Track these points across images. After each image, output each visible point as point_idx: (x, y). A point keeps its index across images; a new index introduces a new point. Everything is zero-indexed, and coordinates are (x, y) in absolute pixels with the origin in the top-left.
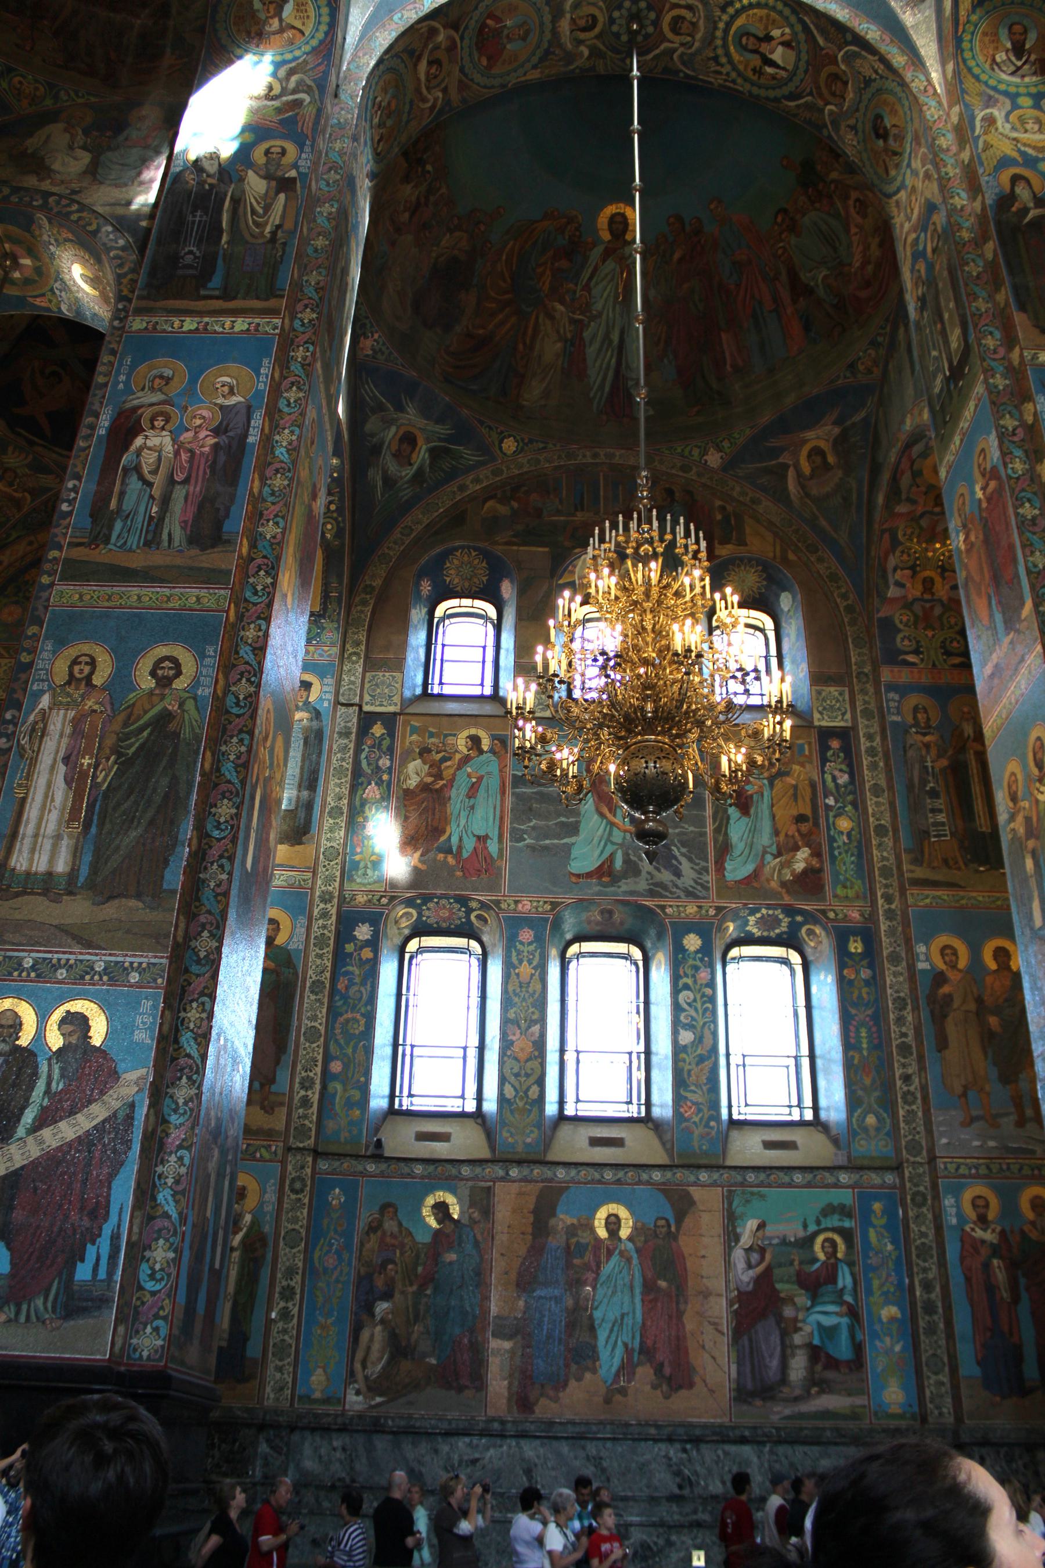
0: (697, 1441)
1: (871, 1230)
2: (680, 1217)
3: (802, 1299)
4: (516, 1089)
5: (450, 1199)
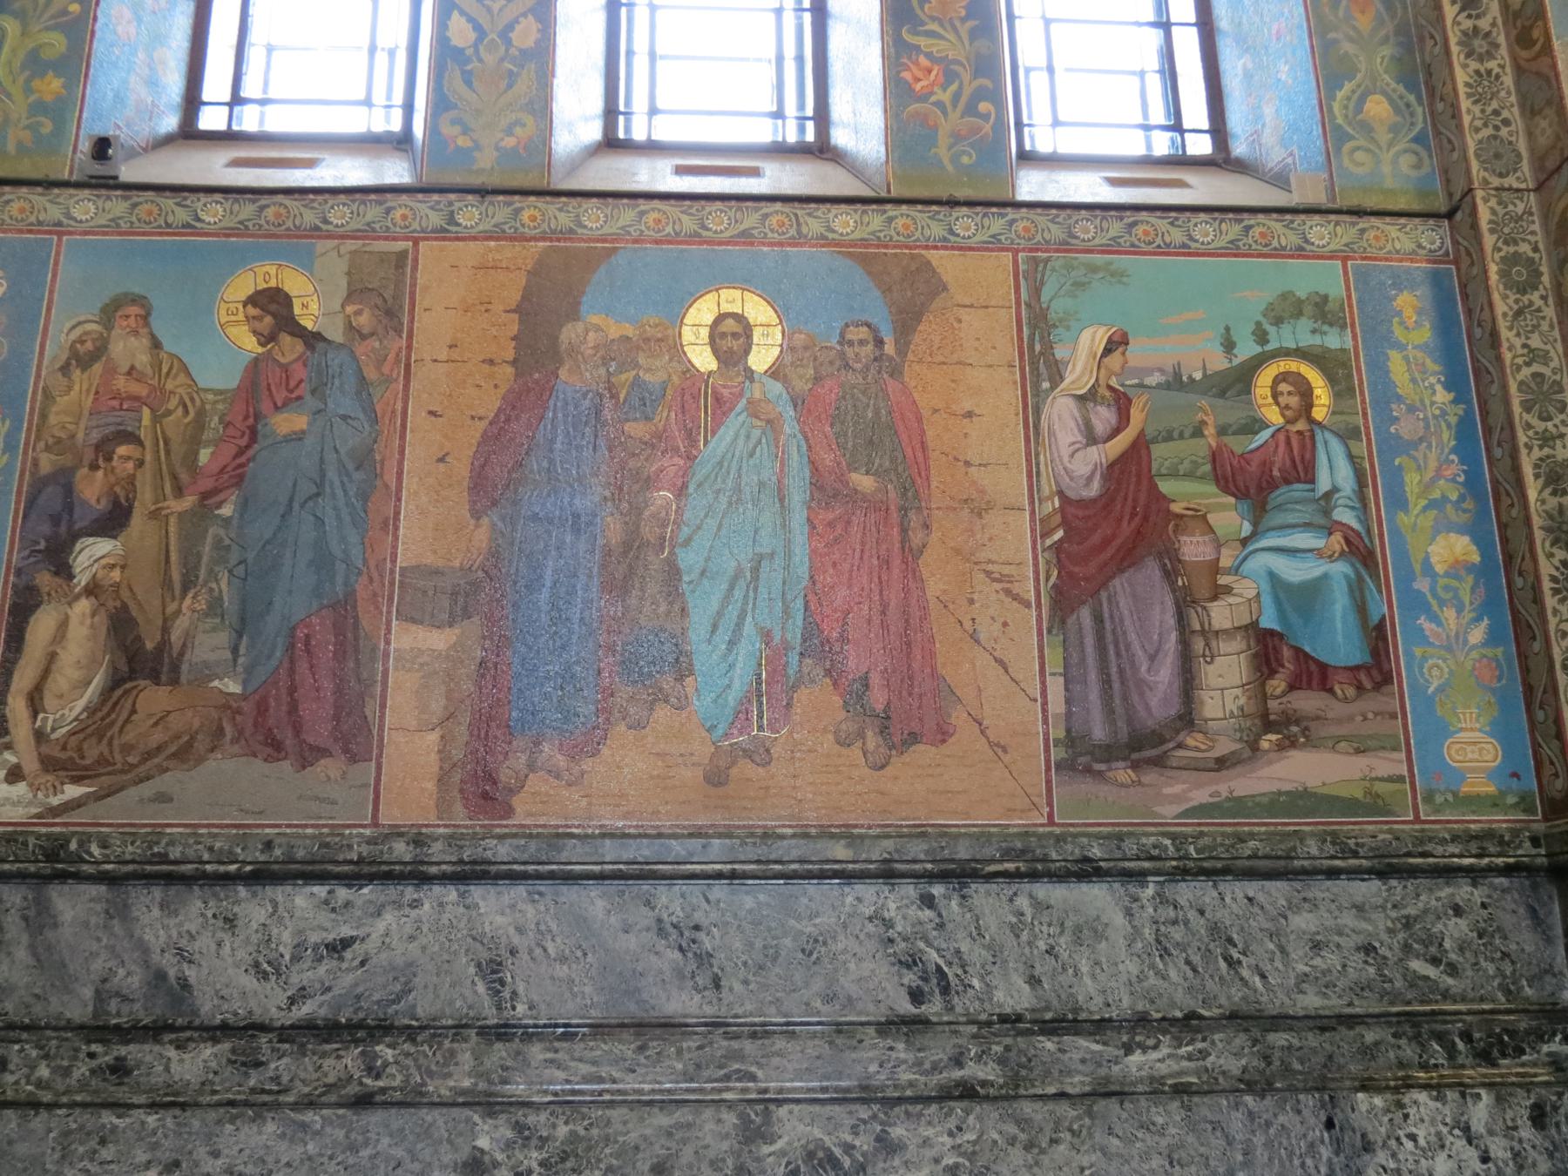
0: (961, 874)
1: (1395, 357)
2: (907, 321)
3: (1229, 518)
4: (478, 28)
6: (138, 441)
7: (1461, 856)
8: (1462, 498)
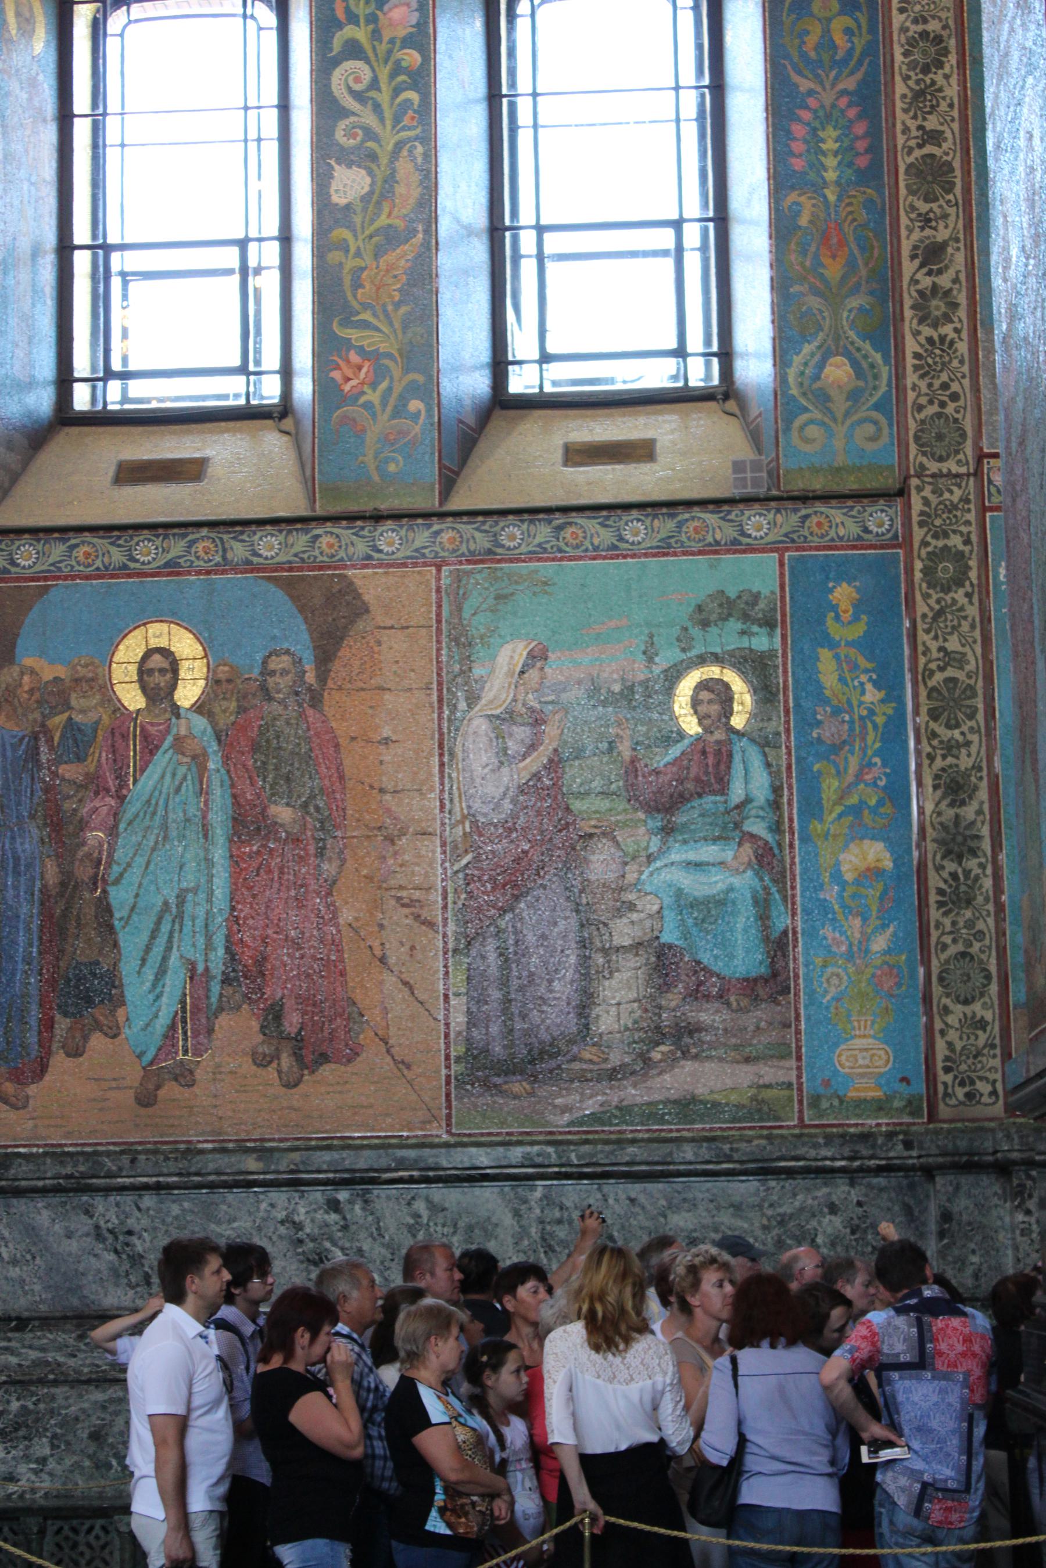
1: (825, 654)
7: (833, 1159)
8: (880, 803)
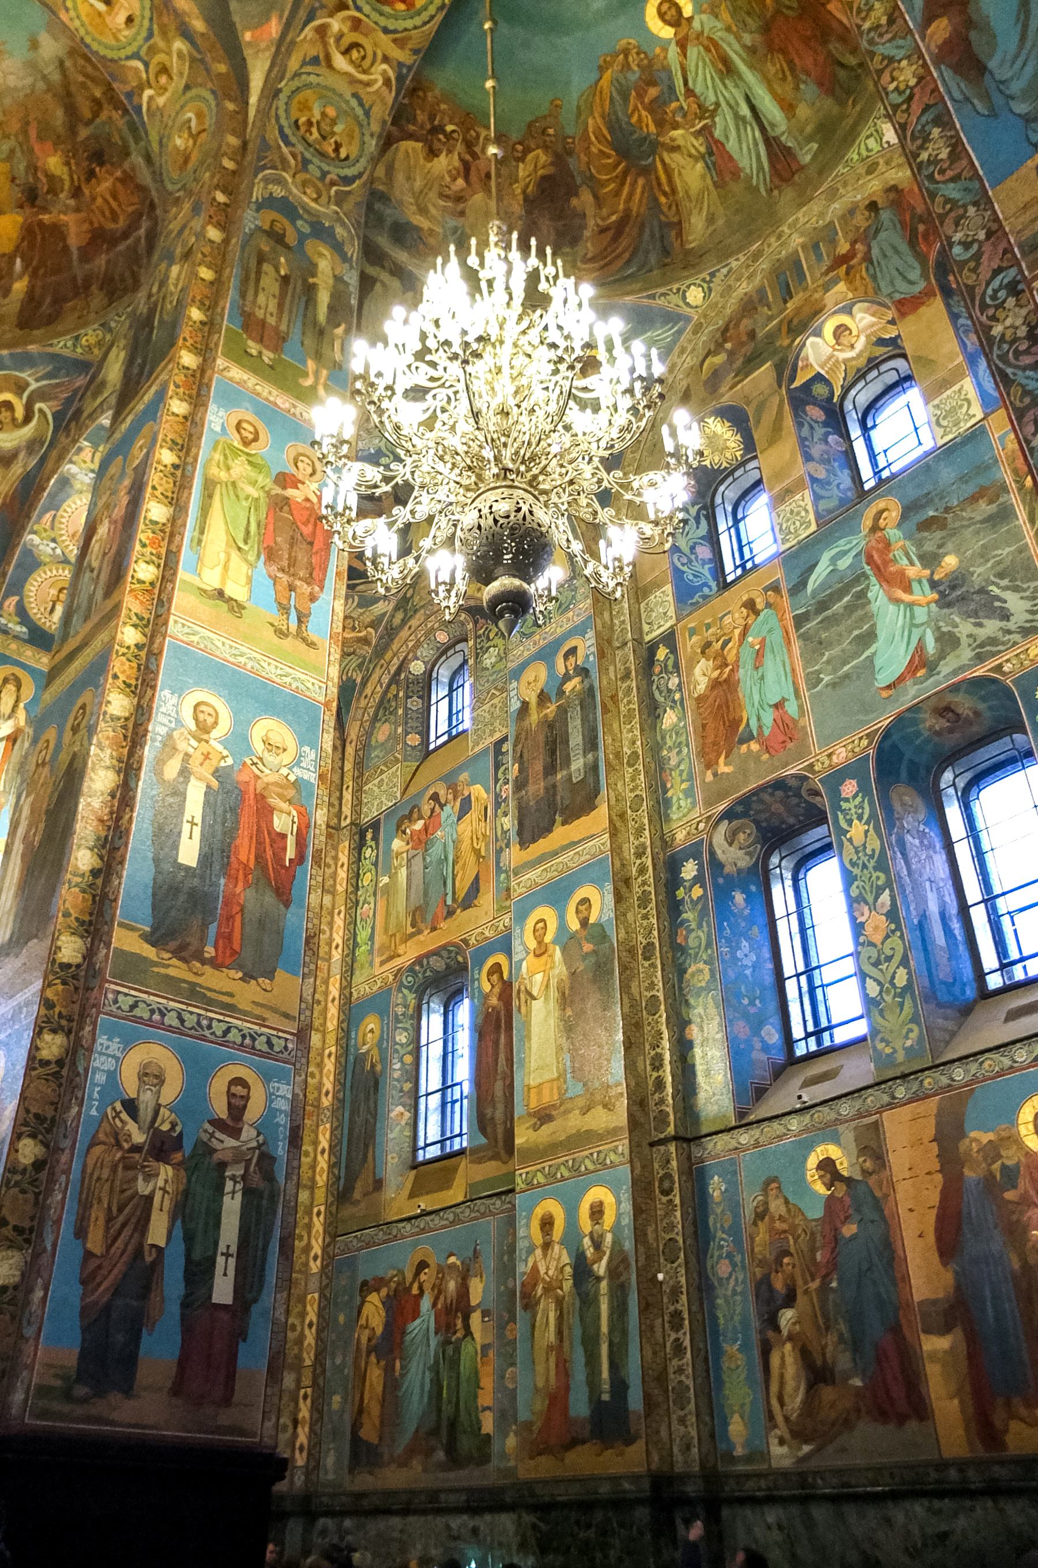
4: (879, 983)
5: (833, 1151)
6: (792, 1255)
